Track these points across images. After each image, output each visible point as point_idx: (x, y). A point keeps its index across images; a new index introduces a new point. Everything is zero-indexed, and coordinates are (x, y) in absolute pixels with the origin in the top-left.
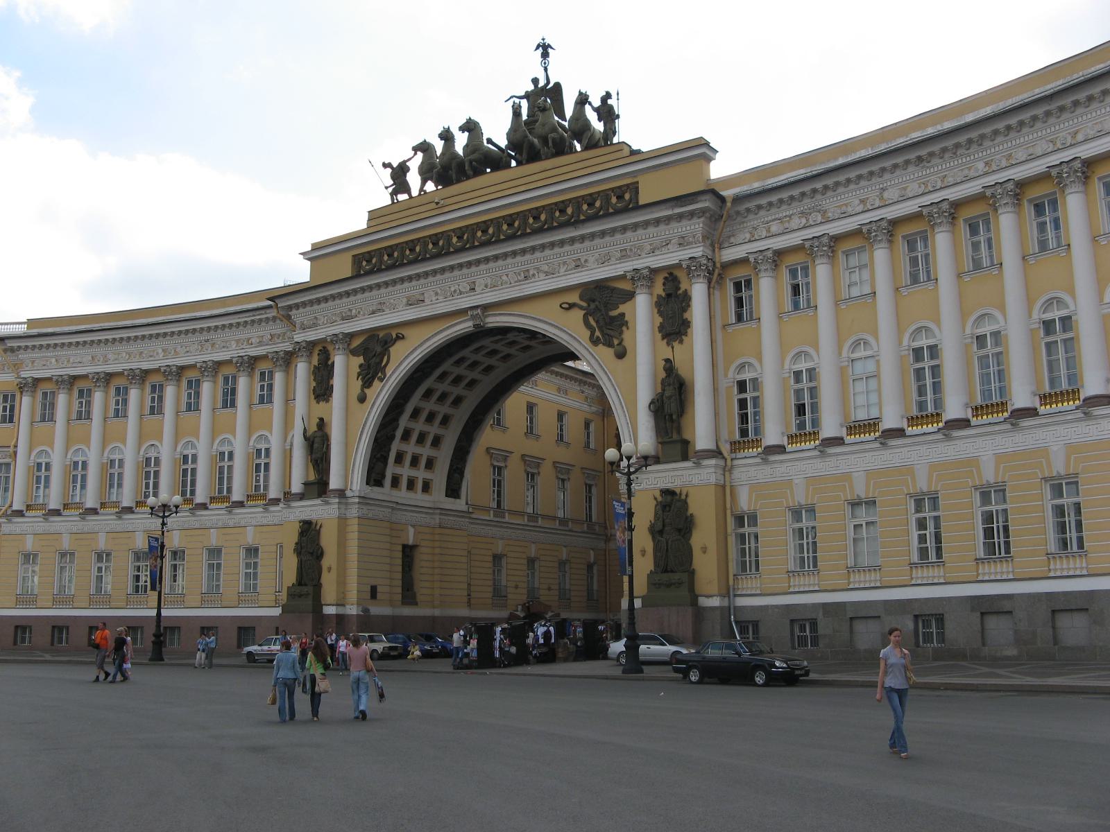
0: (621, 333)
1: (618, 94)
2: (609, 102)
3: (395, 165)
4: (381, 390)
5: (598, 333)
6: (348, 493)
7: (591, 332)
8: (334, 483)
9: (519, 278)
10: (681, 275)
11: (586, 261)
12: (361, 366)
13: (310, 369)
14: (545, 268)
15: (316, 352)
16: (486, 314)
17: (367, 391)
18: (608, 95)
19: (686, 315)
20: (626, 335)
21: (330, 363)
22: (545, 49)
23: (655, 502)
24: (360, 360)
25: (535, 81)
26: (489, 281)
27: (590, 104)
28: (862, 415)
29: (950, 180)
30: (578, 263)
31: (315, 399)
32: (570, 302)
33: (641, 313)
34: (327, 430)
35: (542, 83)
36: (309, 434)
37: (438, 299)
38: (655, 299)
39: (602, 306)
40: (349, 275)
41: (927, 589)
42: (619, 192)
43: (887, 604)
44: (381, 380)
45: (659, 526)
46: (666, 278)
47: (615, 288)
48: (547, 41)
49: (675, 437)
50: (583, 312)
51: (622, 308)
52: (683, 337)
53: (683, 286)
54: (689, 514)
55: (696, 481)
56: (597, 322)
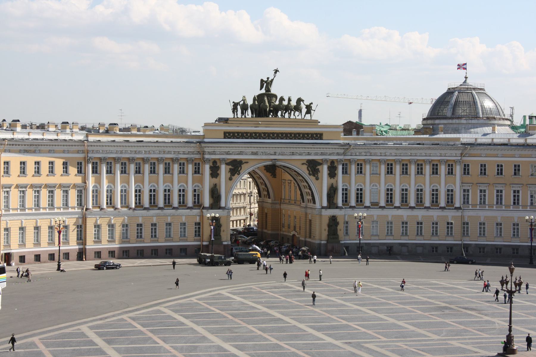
8: (223, 204)
12: (230, 169)
18: (312, 103)
19: (336, 172)
20: (319, 174)
22: (276, 71)
25: (268, 78)
28: (372, 201)
29: (402, 155)
33: (325, 170)
34: (218, 187)
41: (389, 241)
42: (317, 134)
43: (380, 243)
44: (238, 174)
51: (318, 167)
55: (339, 214)
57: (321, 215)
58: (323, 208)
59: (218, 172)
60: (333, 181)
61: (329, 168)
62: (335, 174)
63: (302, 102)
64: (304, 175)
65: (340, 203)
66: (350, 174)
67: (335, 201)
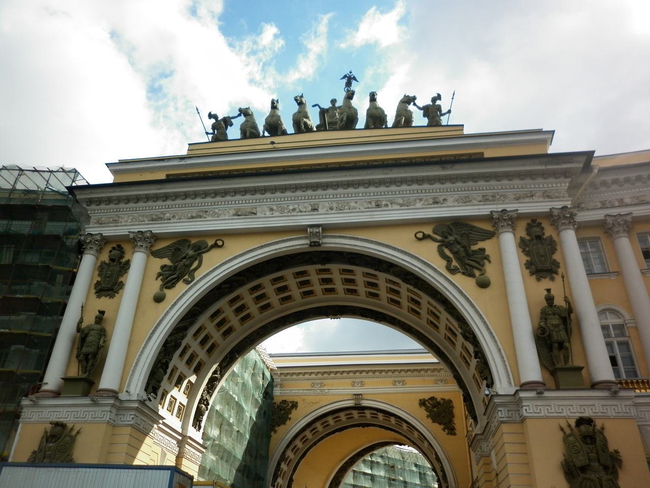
0: (483, 265)
1: (454, 94)
2: (438, 102)
3: (220, 118)
4: (187, 292)
5: (455, 263)
6: (123, 396)
7: (448, 261)
8: (108, 380)
9: (370, 206)
10: (545, 224)
11: (445, 200)
12: (163, 267)
13: (96, 264)
14: (401, 201)
15: (109, 248)
16: (323, 234)
17: (166, 291)
18: (439, 97)
19: (557, 257)
21: (121, 260)
22: (350, 79)
23: (561, 435)
24: (166, 261)
25: (333, 101)
26: (335, 205)
27: (415, 104)
30: (437, 200)
31: (96, 293)
32: (426, 233)
35: (337, 105)
36: (84, 325)
37: (273, 214)
38: (519, 241)
39: (462, 243)
40: (239, 138)
44: (187, 282)
45: (580, 460)
46: (528, 224)
47: (474, 227)
48: (354, 74)
49: (570, 364)
50: (437, 244)
51: (481, 245)
52: (554, 275)
53: (549, 232)
54: (611, 449)
55: (611, 412)
56: (455, 253)
57: (523, 420)
58: (526, 386)
59: (121, 279)
60: (546, 283)
61: (523, 245)
62: (557, 265)
63: (411, 107)
64: (428, 275)
65: (603, 370)
66: (619, 273)
67: (577, 362)
